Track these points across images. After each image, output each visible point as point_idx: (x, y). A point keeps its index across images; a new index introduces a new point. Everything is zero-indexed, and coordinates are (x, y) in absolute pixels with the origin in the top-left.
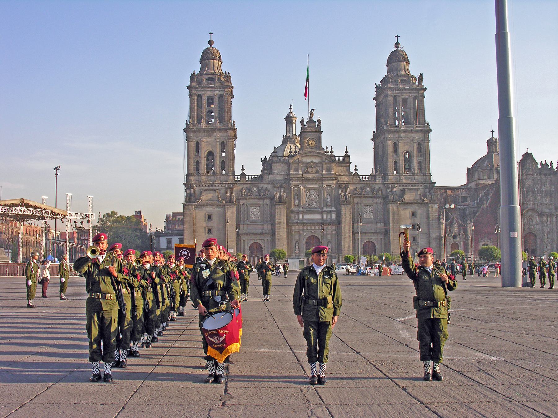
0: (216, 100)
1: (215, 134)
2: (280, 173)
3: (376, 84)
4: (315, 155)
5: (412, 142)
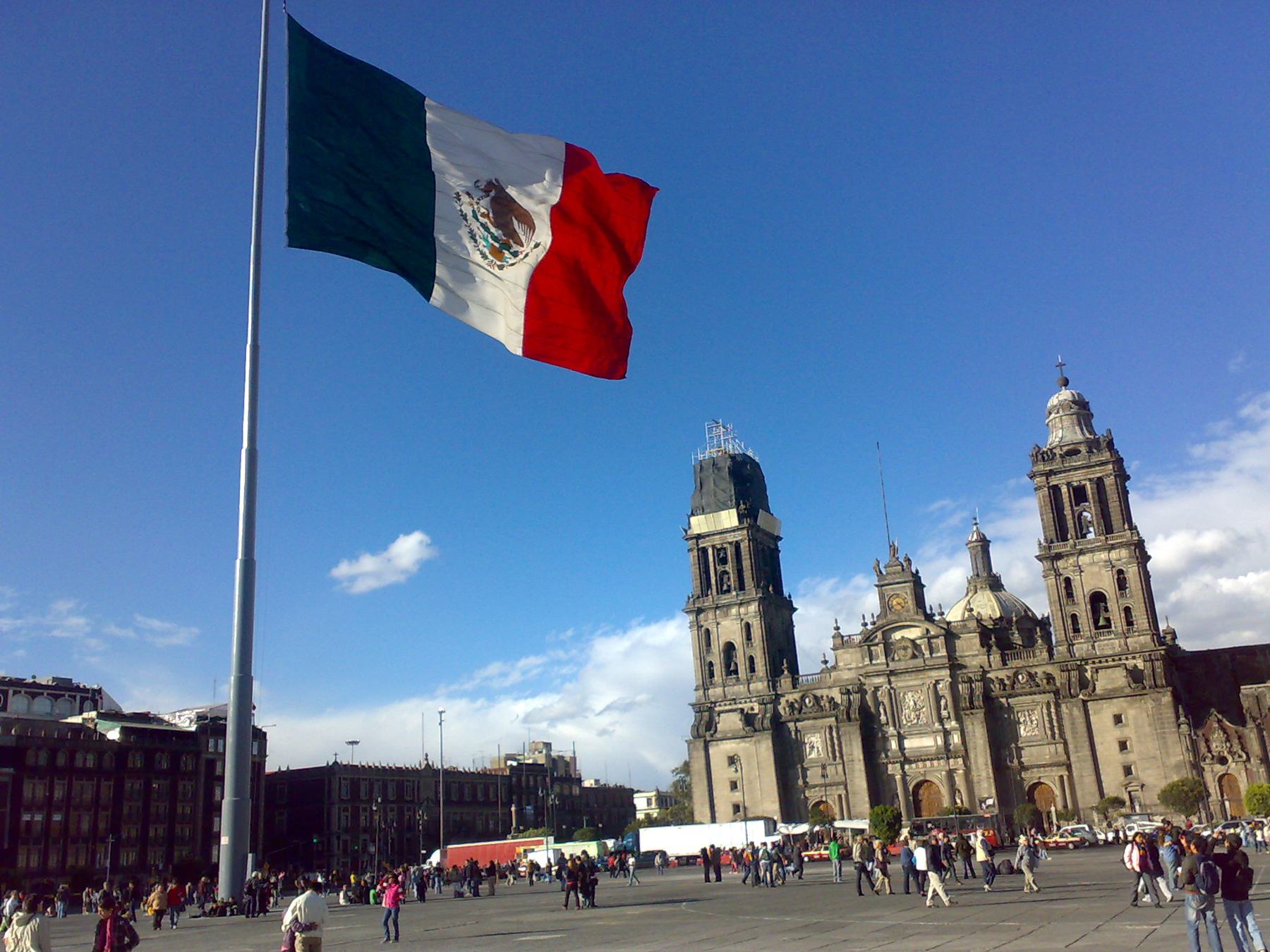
0: (730, 552)
1: (734, 611)
5: (1103, 571)
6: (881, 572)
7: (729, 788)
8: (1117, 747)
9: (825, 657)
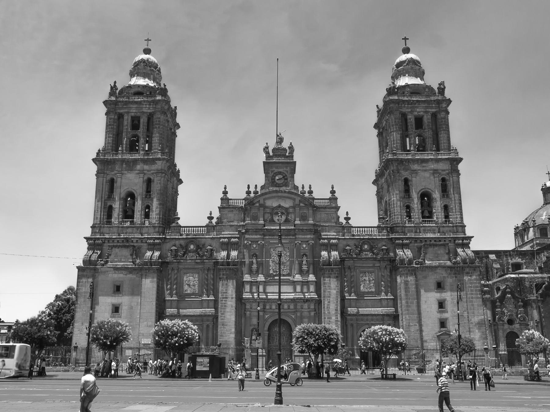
0: (143, 120)
1: (138, 167)
2: (232, 224)
3: (377, 106)
4: (285, 197)
5: (432, 177)
6: (269, 153)
7: (111, 312)
8: (436, 306)
9: (211, 214)
